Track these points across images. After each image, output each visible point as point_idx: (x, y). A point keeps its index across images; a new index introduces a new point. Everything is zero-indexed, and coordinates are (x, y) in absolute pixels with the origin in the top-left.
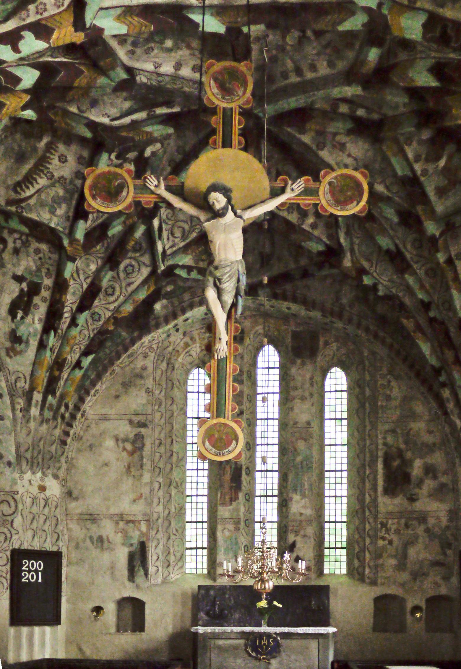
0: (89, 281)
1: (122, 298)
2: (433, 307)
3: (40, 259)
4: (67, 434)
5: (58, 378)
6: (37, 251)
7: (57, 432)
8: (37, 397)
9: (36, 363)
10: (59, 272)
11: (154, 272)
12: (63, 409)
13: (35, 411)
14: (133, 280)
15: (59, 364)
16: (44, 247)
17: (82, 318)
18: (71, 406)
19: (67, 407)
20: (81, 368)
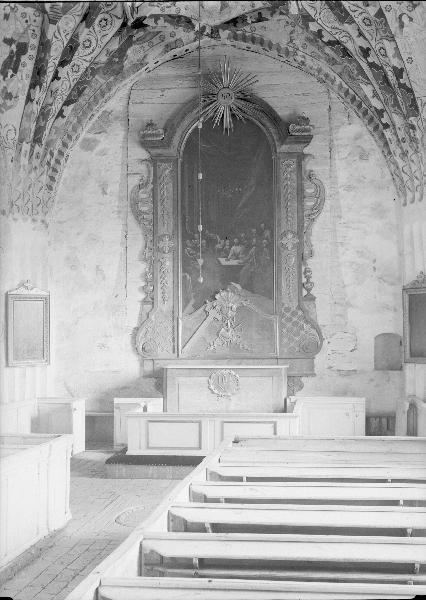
0: (69, 37)
1: (98, 50)
2: (372, 53)
3: (27, 21)
4: (52, 179)
5: (44, 128)
6: (24, 15)
7: (45, 179)
8: (26, 147)
9: (25, 116)
10: (43, 34)
11: (124, 25)
12: (48, 156)
13: (24, 161)
14: (107, 32)
15: (44, 114)
16: (30, 10)
17: (63, 72)
18: (56, 152)
19: (52, 154)
20: (63, 117)
